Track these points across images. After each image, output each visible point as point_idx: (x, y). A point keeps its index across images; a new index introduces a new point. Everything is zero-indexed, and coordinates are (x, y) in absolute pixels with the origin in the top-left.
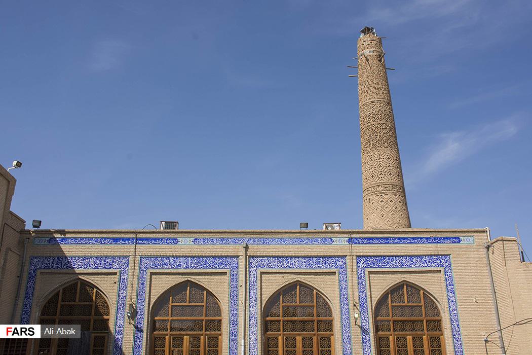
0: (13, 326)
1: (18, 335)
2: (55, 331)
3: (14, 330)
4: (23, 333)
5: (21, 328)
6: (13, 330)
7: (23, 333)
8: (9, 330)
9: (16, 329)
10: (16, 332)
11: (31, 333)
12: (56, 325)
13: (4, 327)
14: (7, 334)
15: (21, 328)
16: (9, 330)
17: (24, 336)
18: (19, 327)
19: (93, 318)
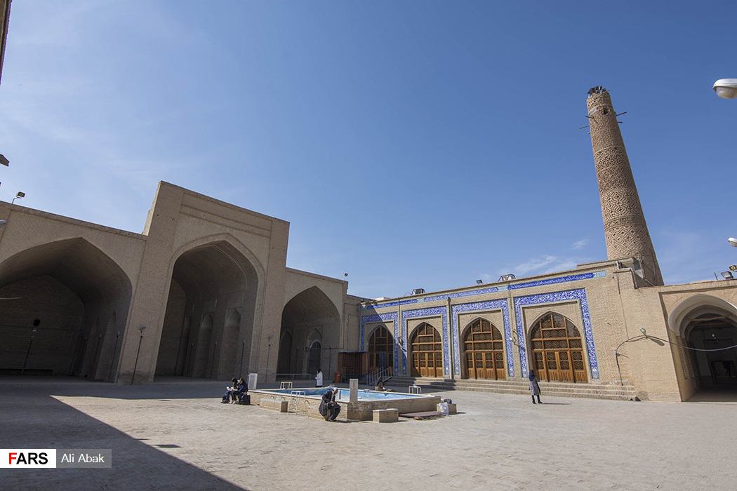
0: (19, 451)
1: (26, 463)
2: (76, 458)
3: (20, 457)
4: (32, 461)
5: (30, 454)
6: (17, 456)
7: (32, 461)
8: (13, 456)
9: (22, 454)
10: (22, 459)
11: (43, 461)
12: (80, 450)
13: (5, 453)
14: (10, 463)
15: (30, 454)
16: (13, 456)
17: (33, 465)
18: (26, 452)
19: (93, 446)
